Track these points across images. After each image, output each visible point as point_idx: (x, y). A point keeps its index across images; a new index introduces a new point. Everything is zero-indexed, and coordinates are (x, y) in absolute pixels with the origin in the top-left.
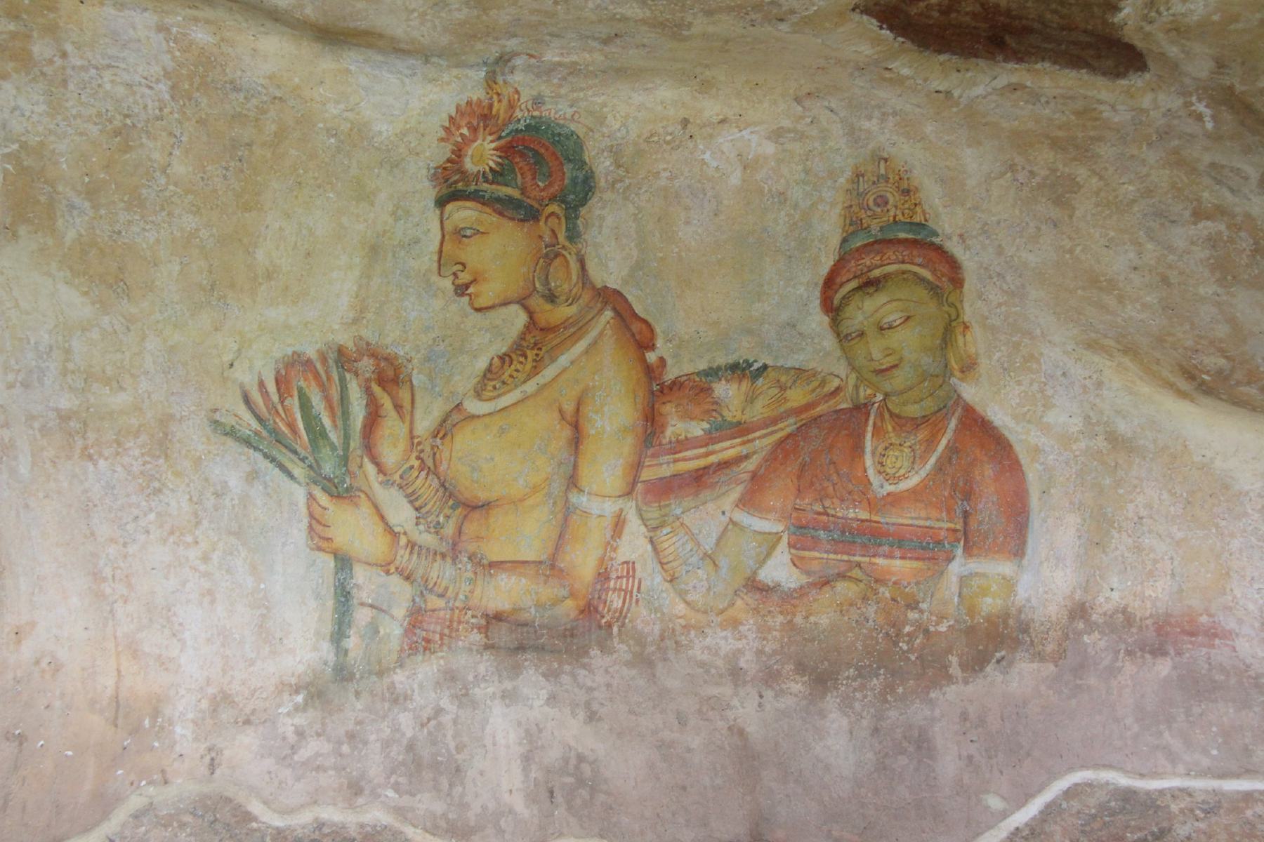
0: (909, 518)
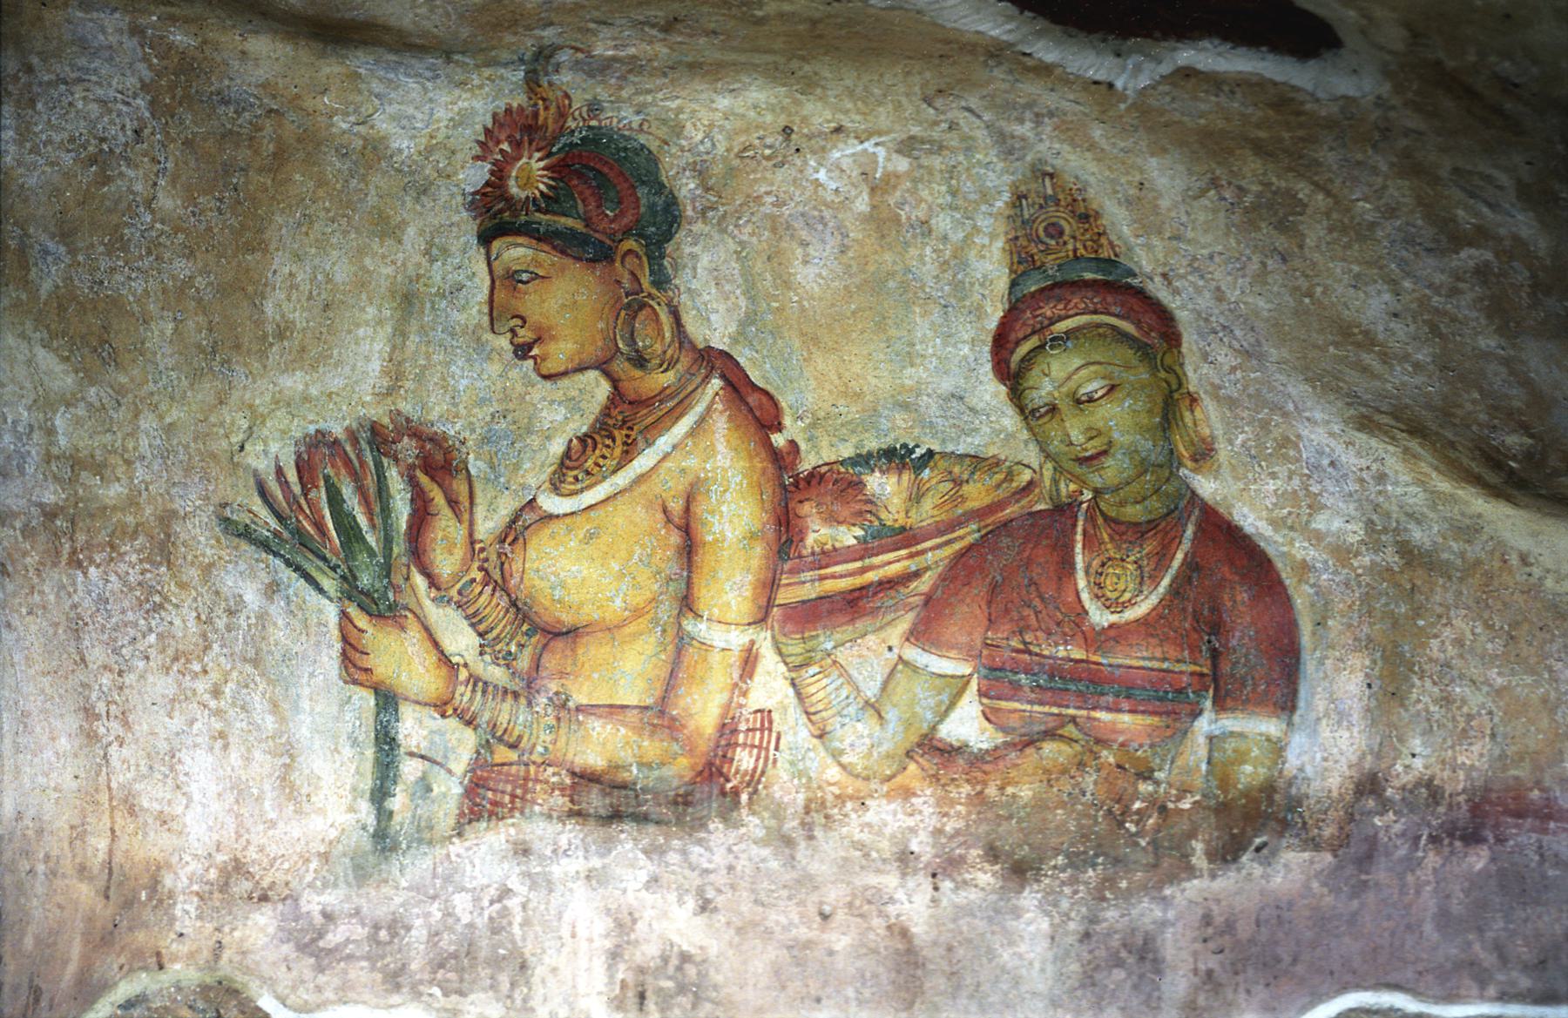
0: (1137, 658)
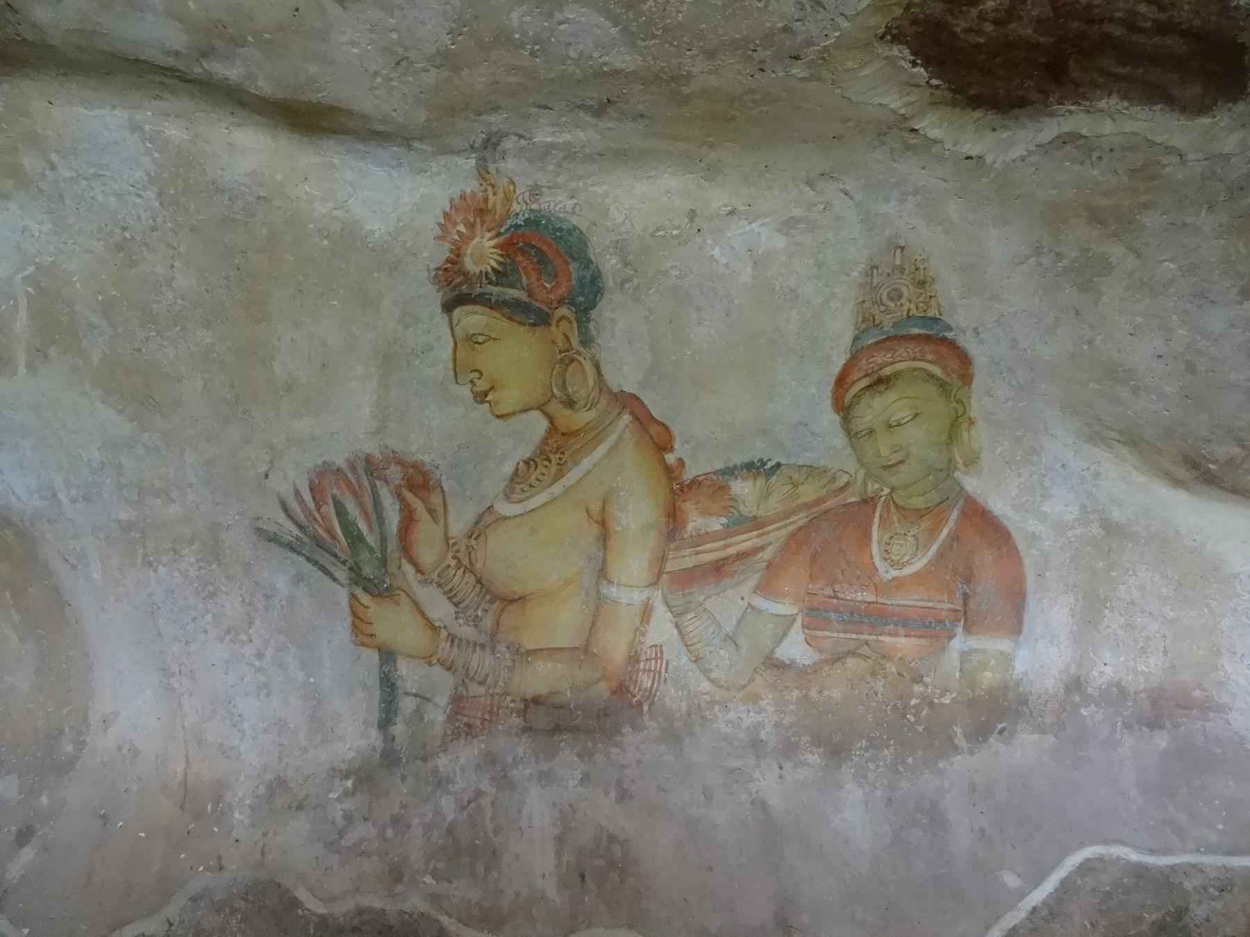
0: (911, 600)
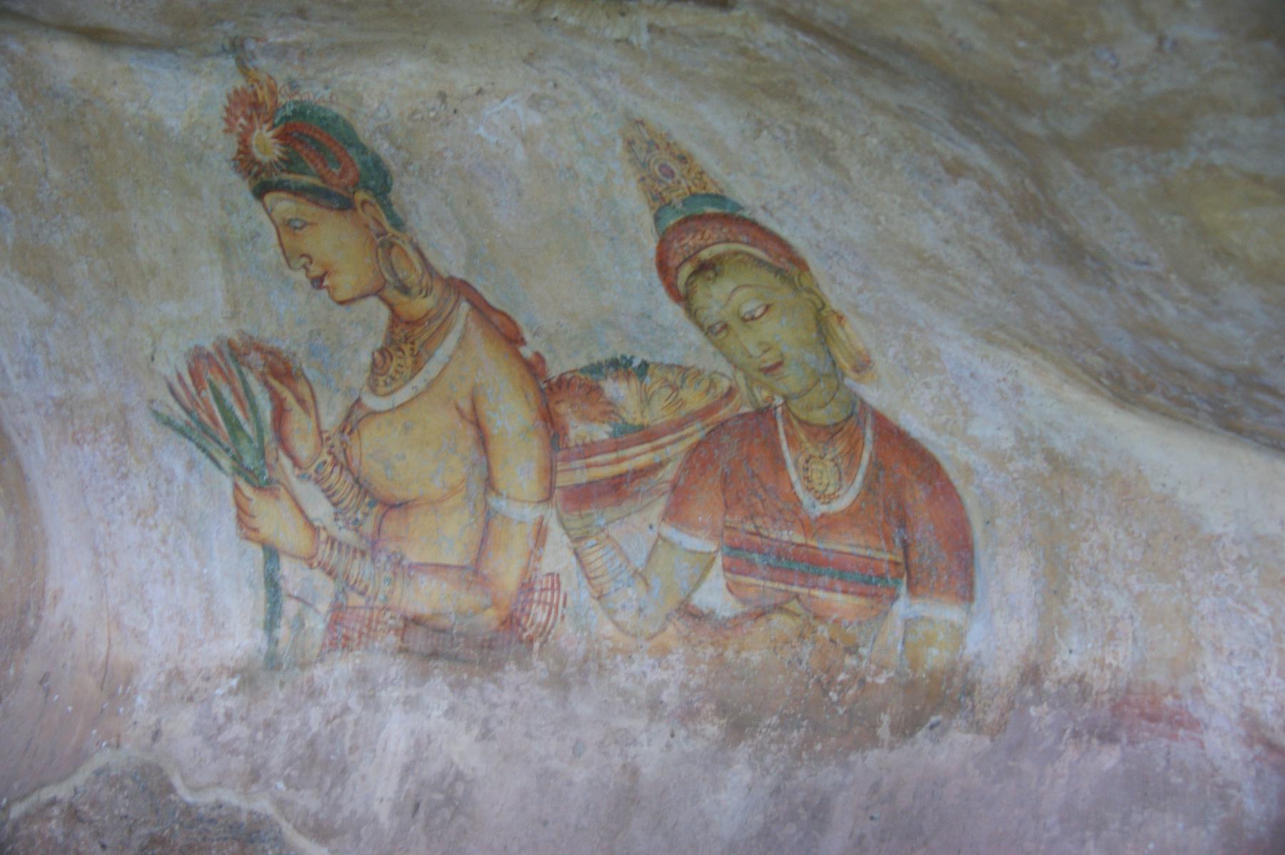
0: (847, 544)
